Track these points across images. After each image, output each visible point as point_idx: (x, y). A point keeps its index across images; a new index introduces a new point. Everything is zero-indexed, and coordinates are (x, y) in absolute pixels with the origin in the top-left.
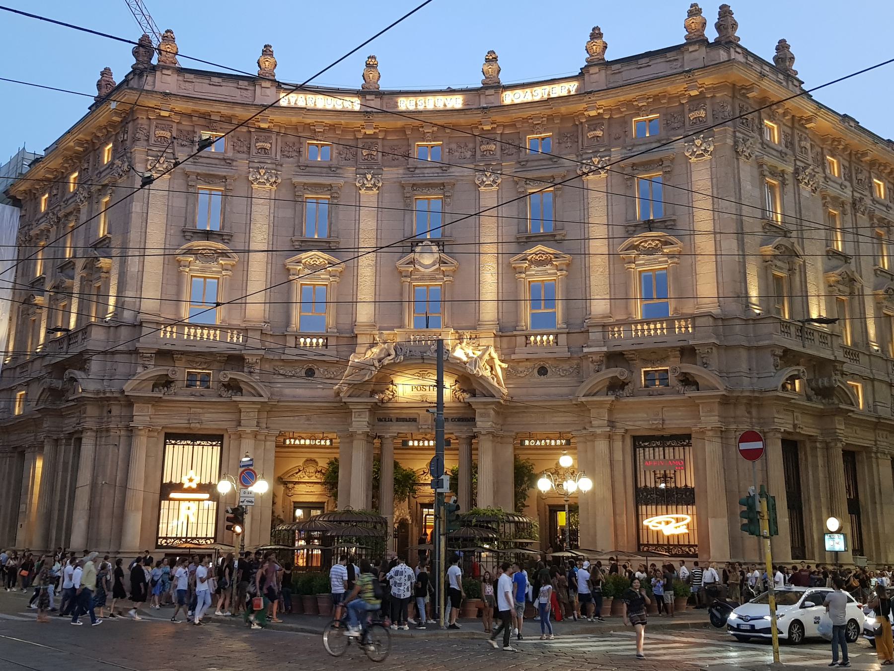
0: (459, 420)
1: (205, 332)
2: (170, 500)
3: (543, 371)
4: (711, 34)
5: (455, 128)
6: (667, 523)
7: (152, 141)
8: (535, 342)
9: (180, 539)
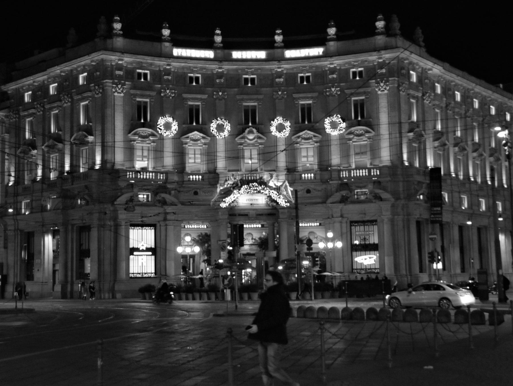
2: (133, 255)
3: (308, 191)
6: (365, 259)
9: (140, 274)
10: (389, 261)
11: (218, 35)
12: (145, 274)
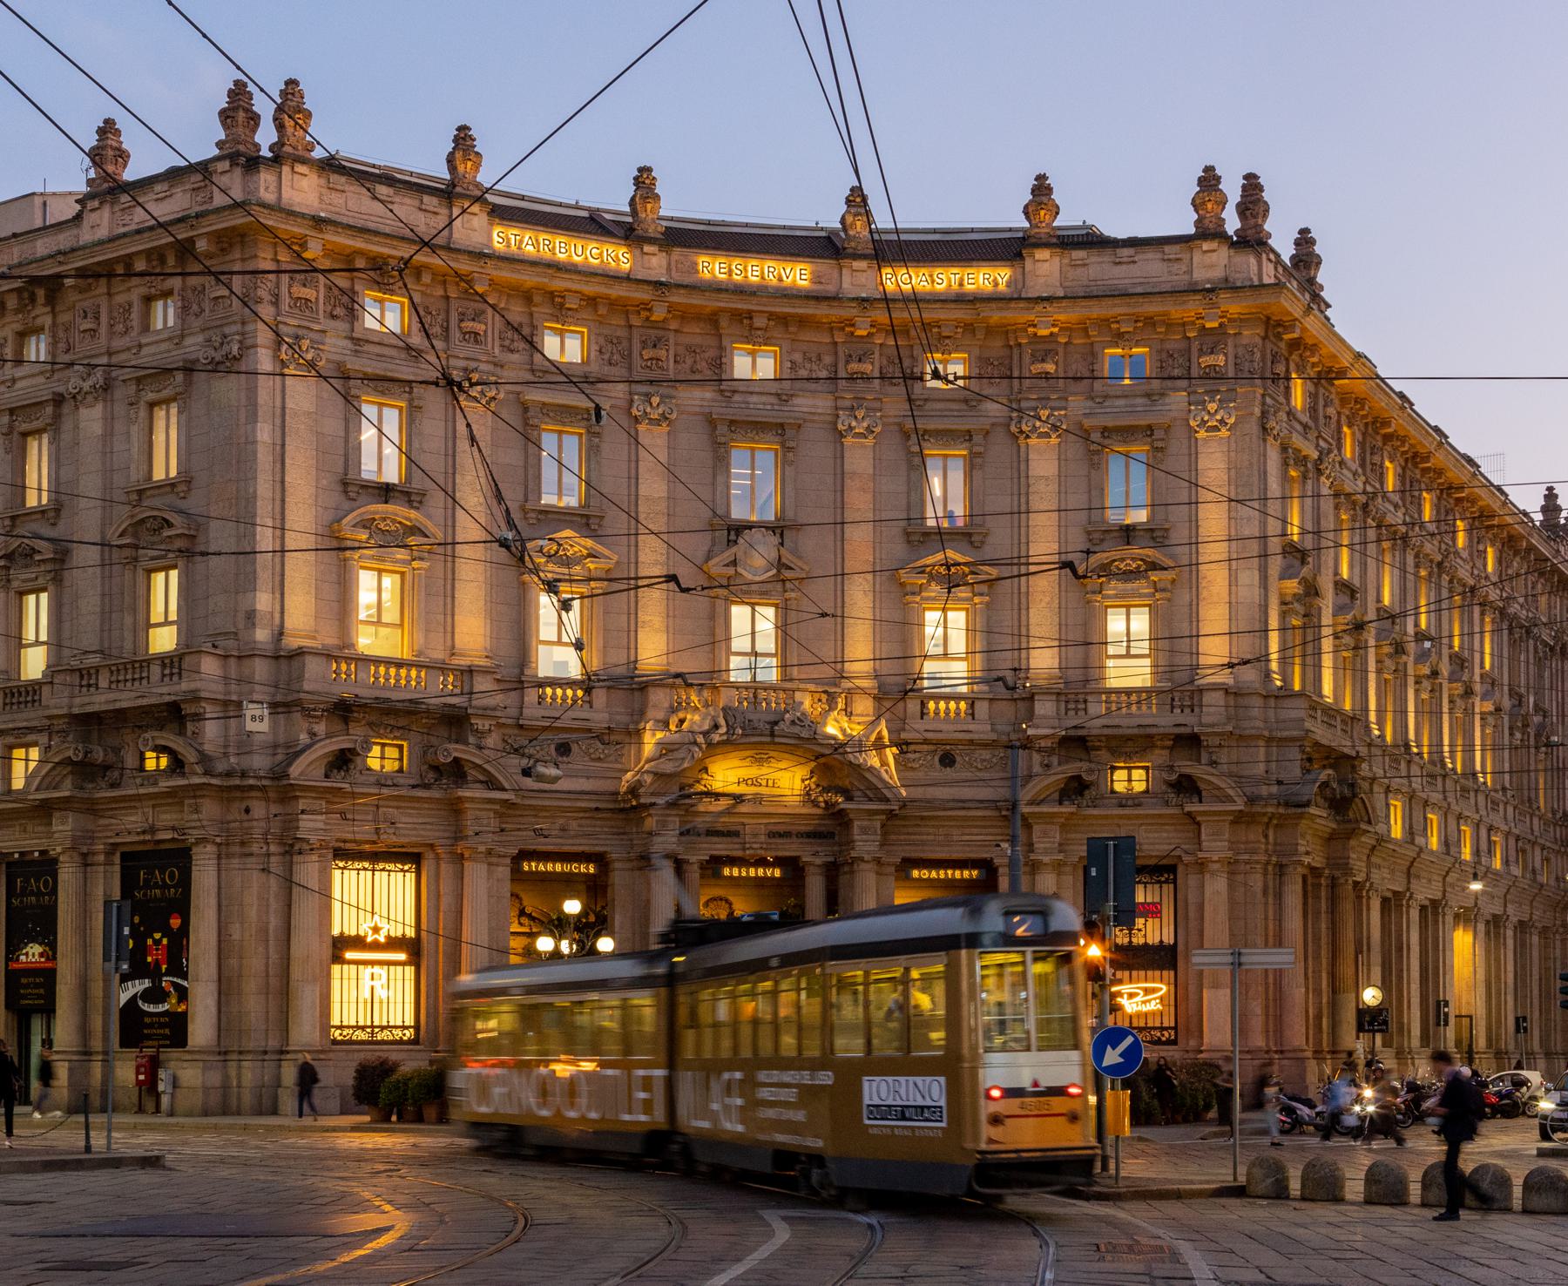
0: (809, 835)
1: (403, 672)
4: (1232, 223)
5: (803, 322)
7: (285, 307)
8: (937, 712)
9: (363, 1028)
12: (382, 1028)
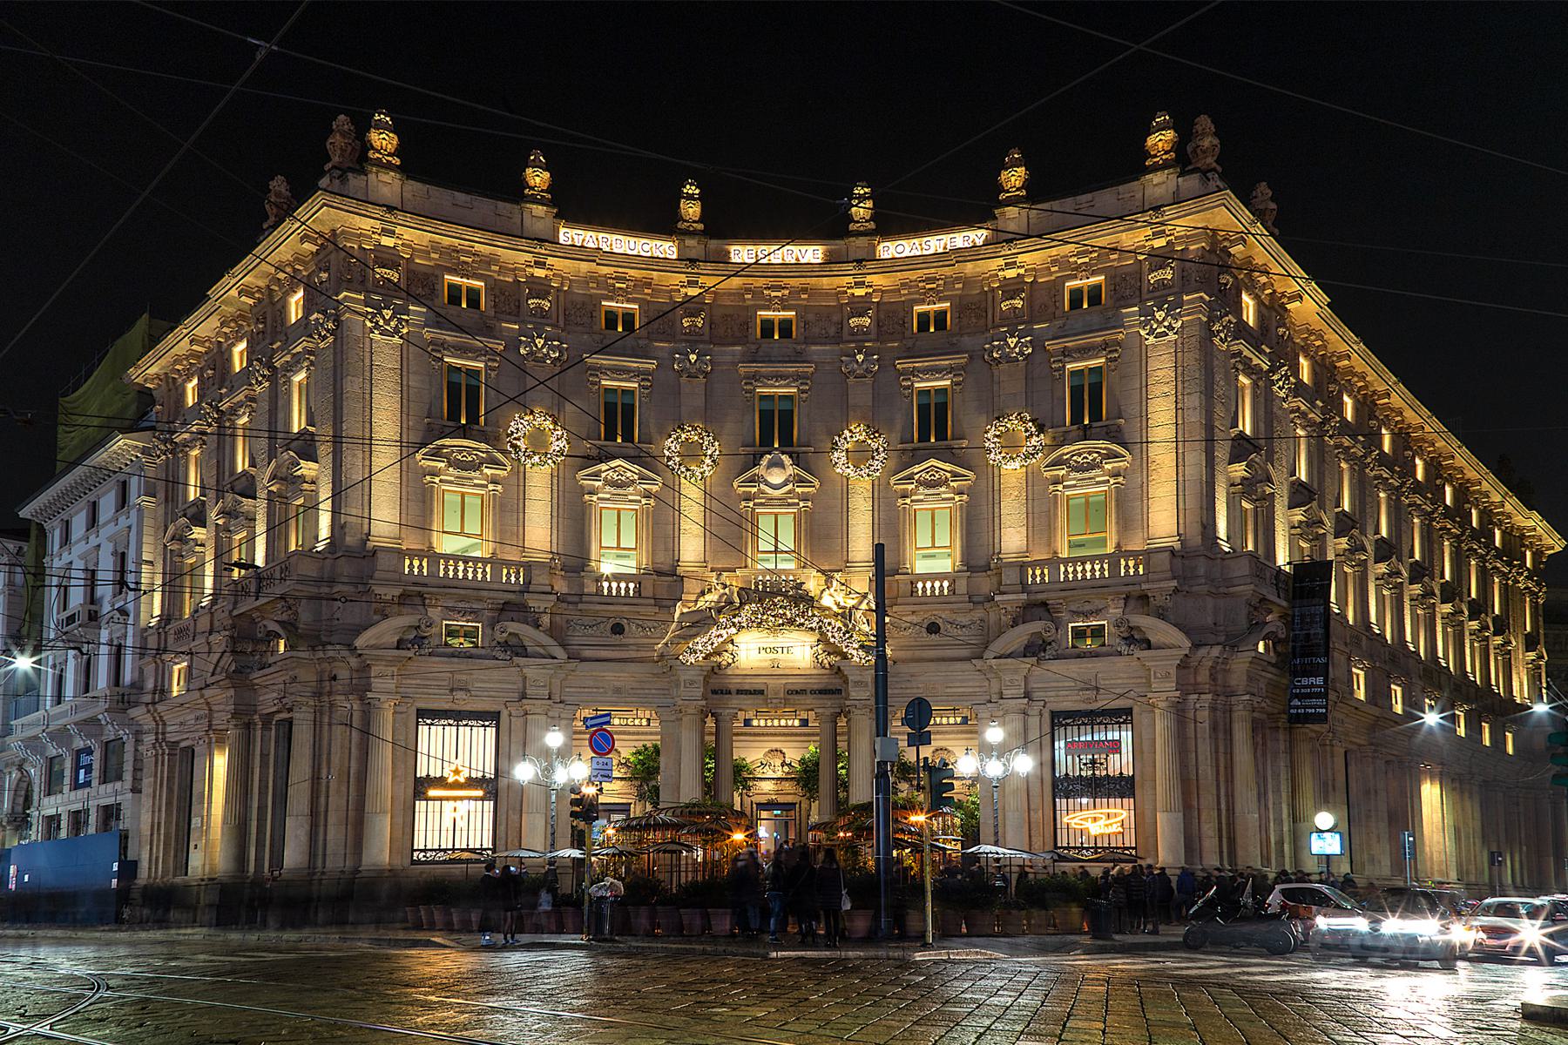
0: (821, 692)
2: (427, 799)
3: (933, 628)
10: (1166, 827)
11: (690, 197)
